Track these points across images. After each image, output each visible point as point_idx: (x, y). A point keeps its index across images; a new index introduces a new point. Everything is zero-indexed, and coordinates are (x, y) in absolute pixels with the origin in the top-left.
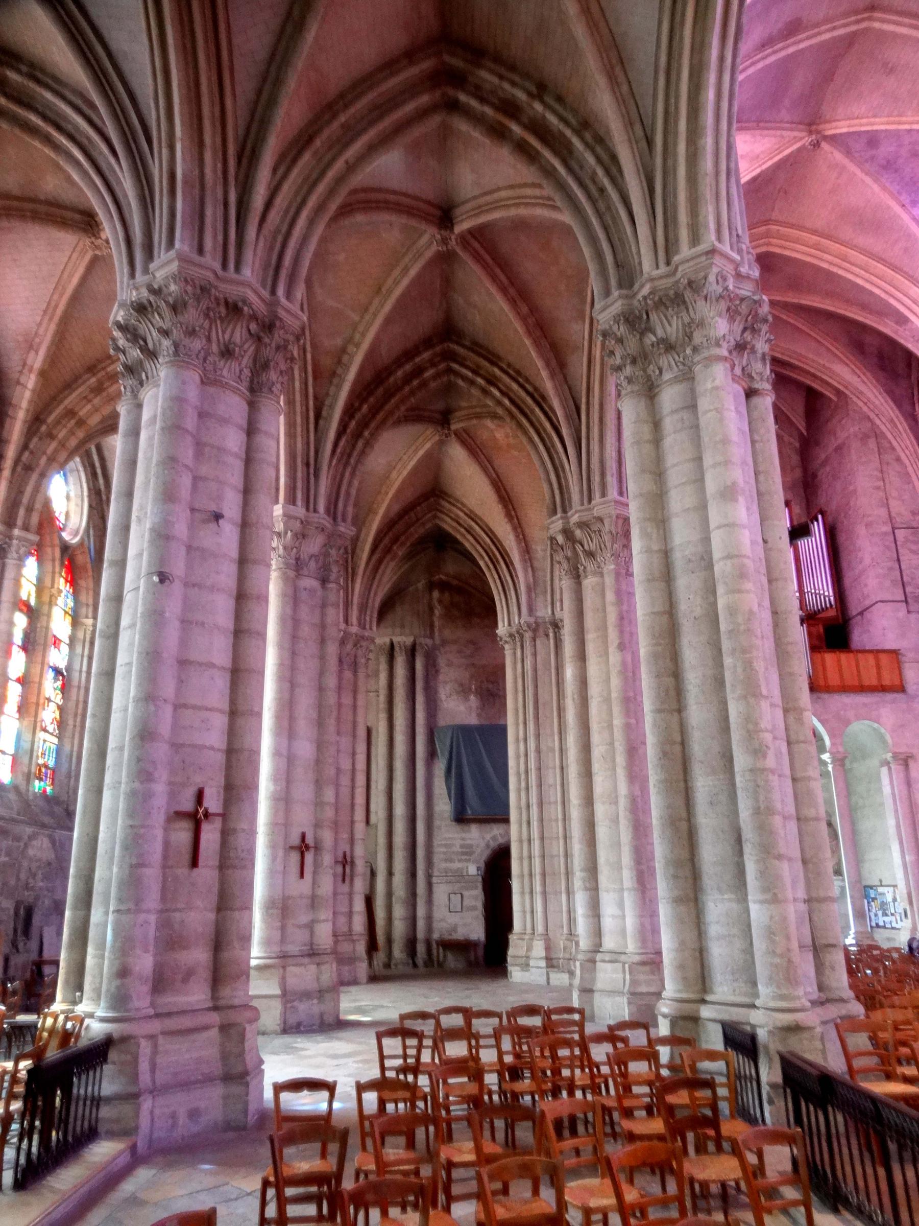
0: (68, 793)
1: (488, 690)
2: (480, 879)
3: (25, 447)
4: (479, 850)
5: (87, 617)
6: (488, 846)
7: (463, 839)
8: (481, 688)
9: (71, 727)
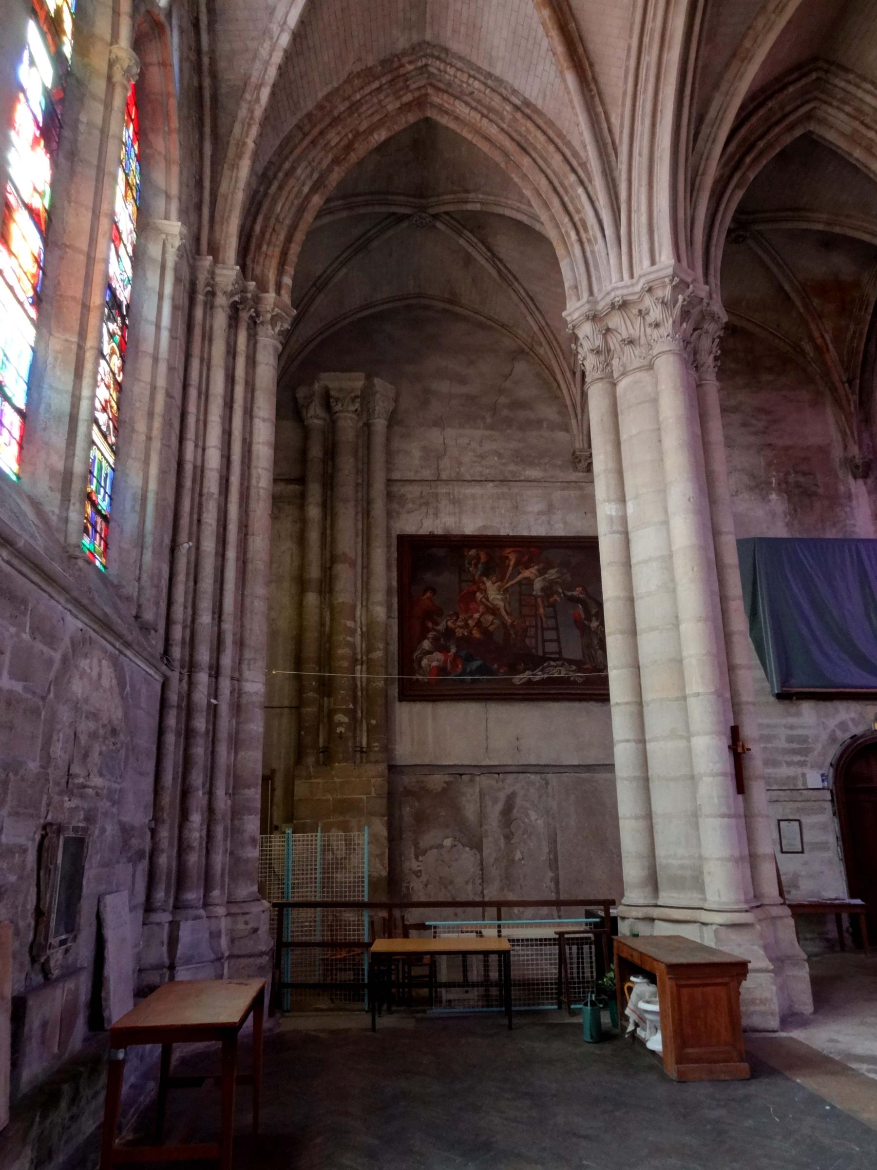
0: (139, 579)
1: (798, 485)
2: (828, 796)
4: (819, 746)
5: (167, 217)
6: (833, 739)
7: (791, 727)
8: (786, 483)
9: (140, 439)
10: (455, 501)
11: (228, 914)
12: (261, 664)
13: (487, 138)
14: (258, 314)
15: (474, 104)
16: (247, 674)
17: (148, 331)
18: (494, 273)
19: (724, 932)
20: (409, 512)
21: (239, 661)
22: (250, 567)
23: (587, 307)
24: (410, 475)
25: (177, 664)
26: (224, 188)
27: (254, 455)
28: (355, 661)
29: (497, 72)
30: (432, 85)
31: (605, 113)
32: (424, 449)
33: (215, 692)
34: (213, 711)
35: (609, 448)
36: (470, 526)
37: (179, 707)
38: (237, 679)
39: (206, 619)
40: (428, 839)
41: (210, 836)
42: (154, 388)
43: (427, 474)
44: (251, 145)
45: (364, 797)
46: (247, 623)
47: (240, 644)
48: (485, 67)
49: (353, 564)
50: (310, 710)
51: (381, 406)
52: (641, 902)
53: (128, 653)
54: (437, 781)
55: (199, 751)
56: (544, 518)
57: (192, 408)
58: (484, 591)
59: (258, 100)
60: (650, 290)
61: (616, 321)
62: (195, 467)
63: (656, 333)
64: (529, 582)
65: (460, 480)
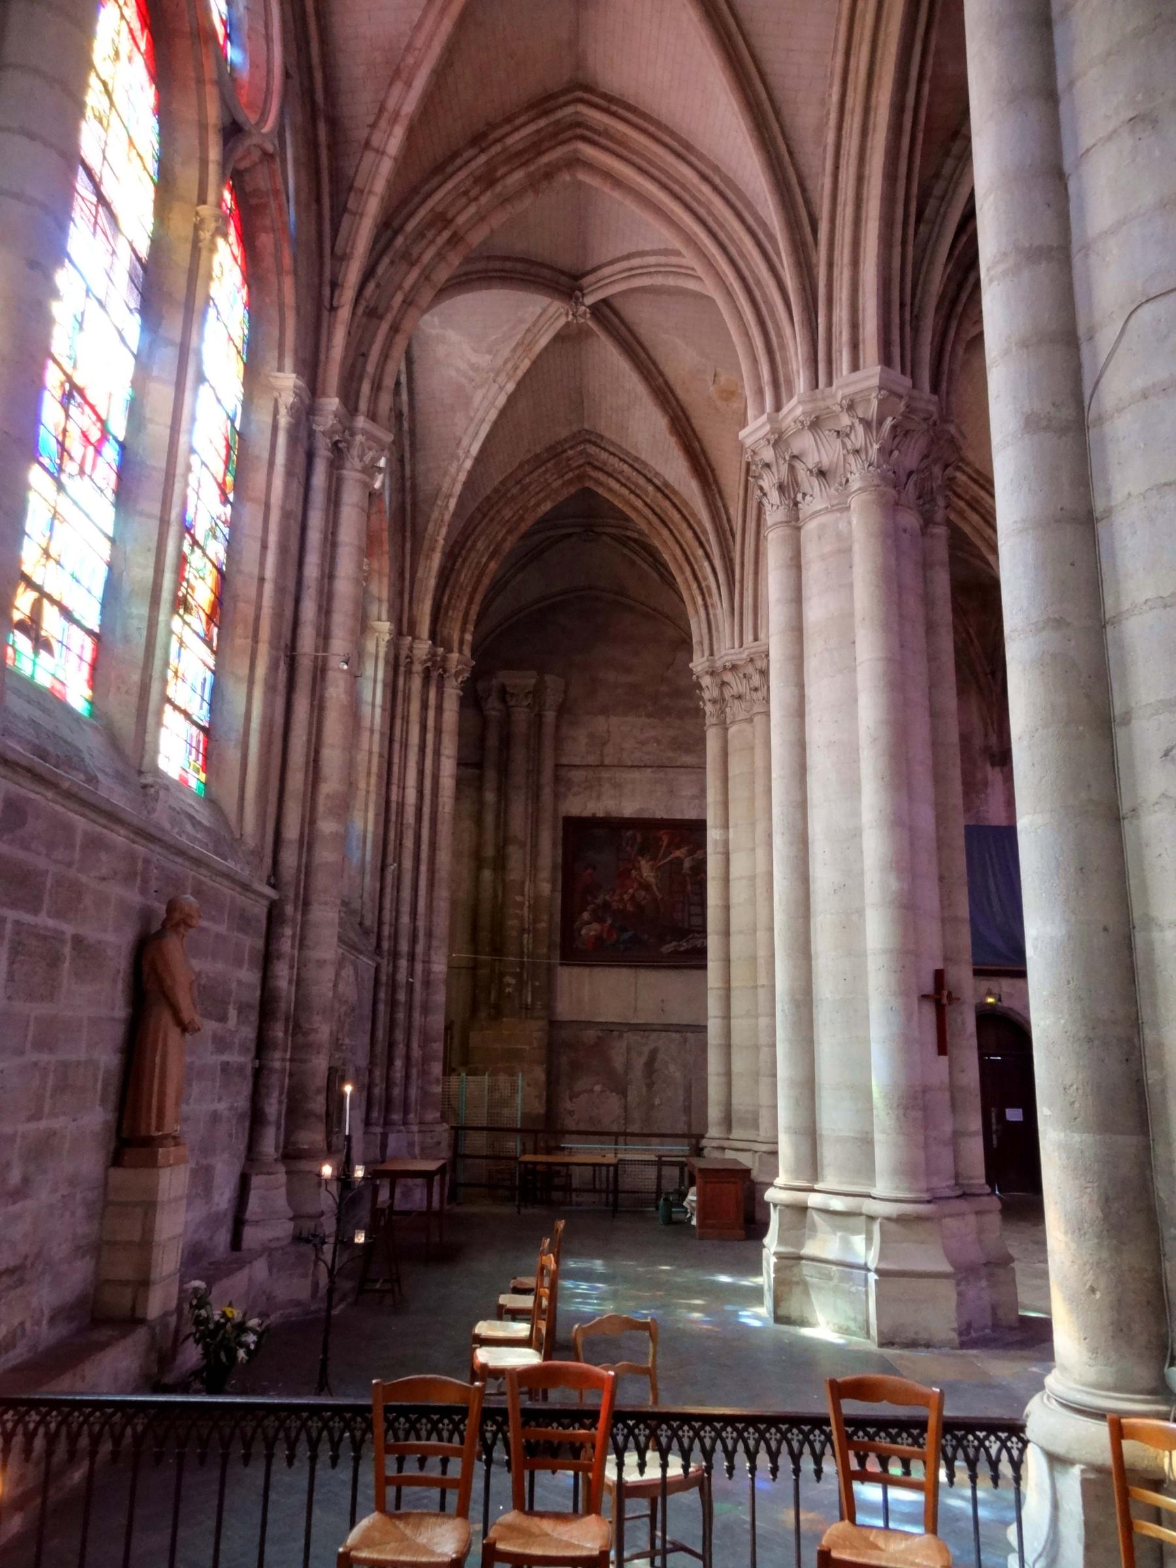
0: (361, 897)
3: (368, 274)
5: (379, 620)
10: (617, 786)
11: (420, 1132)
12: (444, 950)
13: (635, 509)
14: (445, 671)
15: (623, 480)
16: (434, 958)
17: (366, 710)
18: (655, 575)
19: (765, 1156)
20: (575, 795)
21: (429, 948)
22: (437, 875)
23: (707, 664)
24: (577, 761)
25: (386, 954)
26: (420, 574)
27: (441, 786)
28: (523, 930)
29: (643, 457)
30: (589, 463)
31: (725, 506)
32: (591, 736)
33: (411, 973)
34: (410, 987)
35: (718, 784)
36: (629, 808)
37: (387, 984)
38: (427, 961)
39: (405, 919)
40: (581, 1084)
41: (407, 1077)
42: (370, 753)
43: (592, 759)
44: (441, 542)
45: (527, 1048)
46: (435, 919)
47: (430, 935)
48: (633, 452)
49: (522, 845)
50: (483, 972)
51: (552, 698)
52: (717, 1136)
53: (361, 957)
54: (591, 1035)
55: (401, 1016)
56: (697, 801)
57: (396, 760)
58: (639, 869)
59: (447, 507)
60: (752, 660)
61: (728, 677)
62: (398, 803)
63: (755, 695)
64: (679, 861)
65: (621, 766)
